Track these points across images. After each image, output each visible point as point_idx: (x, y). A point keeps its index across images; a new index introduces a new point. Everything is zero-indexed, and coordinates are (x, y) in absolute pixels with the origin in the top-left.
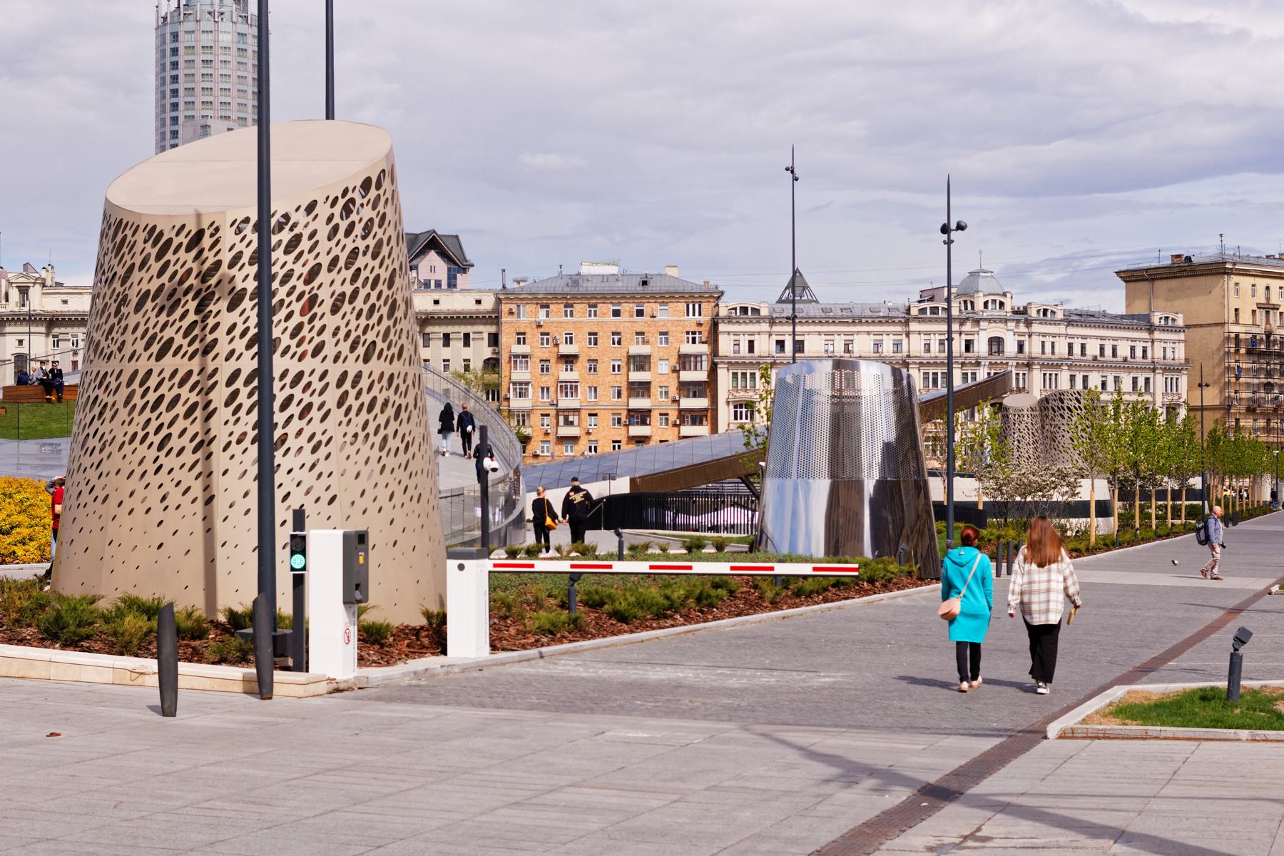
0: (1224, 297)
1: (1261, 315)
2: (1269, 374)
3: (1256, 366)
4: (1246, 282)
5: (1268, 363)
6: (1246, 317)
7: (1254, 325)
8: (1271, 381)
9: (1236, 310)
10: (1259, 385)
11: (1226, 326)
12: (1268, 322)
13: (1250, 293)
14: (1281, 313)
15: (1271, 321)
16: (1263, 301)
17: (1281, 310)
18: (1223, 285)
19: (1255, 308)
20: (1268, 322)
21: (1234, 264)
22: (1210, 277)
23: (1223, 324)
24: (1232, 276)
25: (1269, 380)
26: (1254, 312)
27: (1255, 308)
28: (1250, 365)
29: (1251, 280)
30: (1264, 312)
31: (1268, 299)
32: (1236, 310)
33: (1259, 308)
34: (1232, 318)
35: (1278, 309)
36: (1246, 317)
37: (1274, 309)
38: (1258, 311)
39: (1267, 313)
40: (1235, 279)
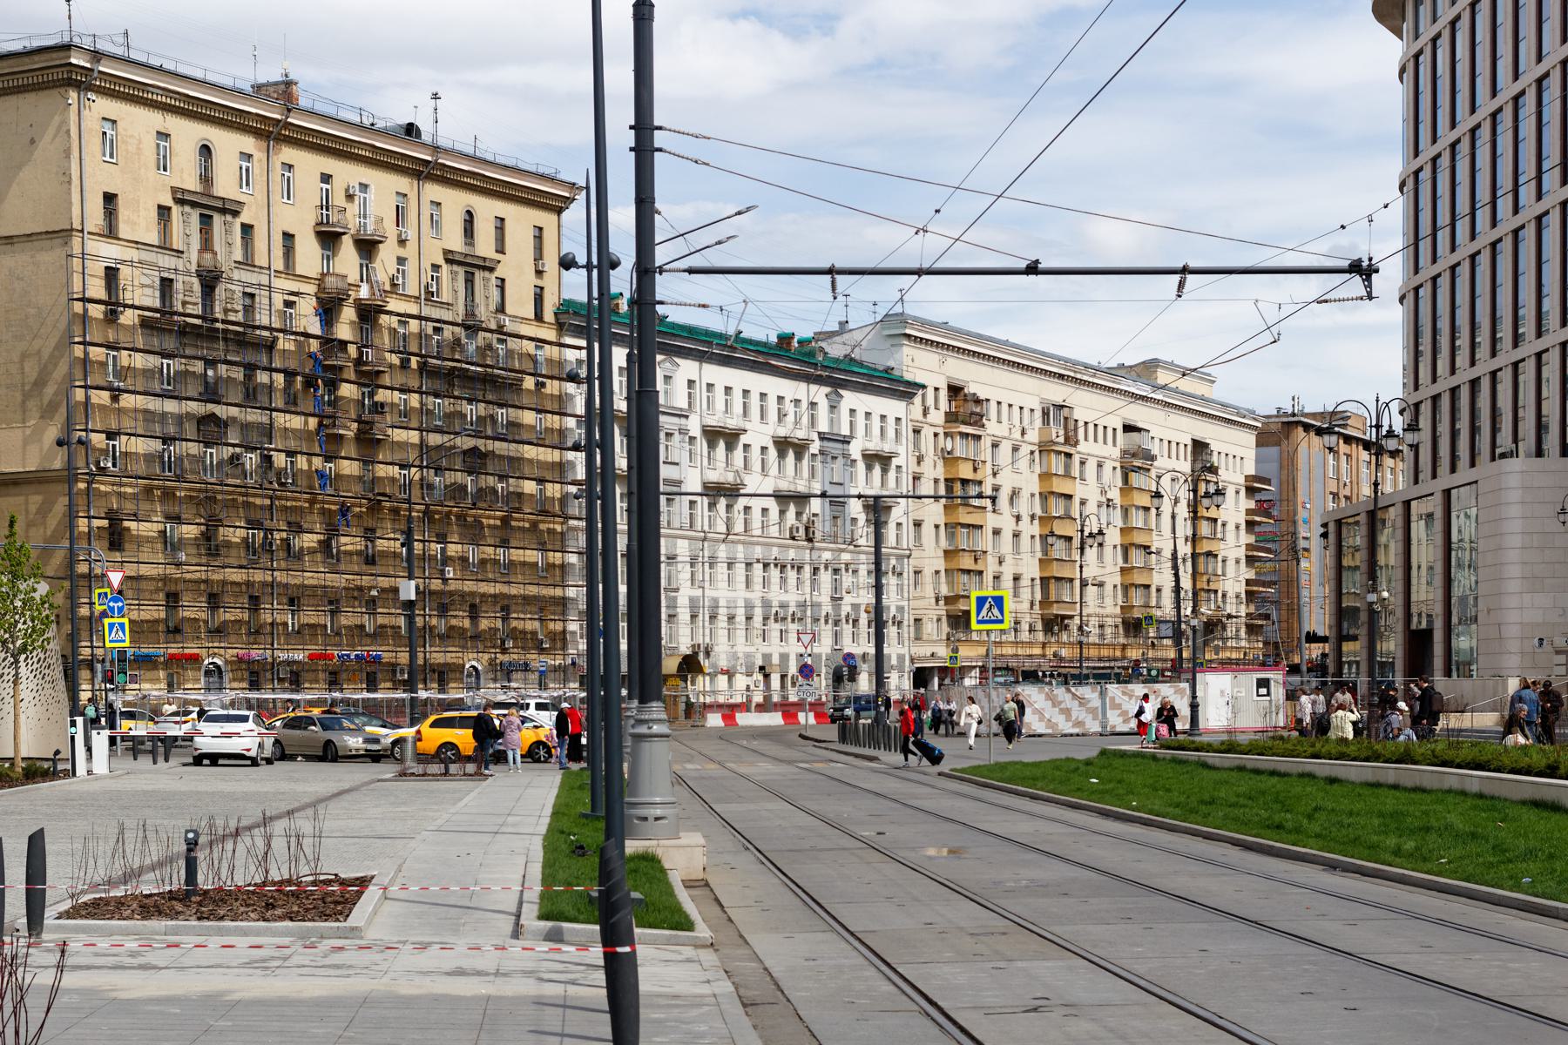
0: (67, 154)
1: (185, 225)
2: (211, 393)
3: (175, 365)
4: (139, 123)
5: (211, 363)
6: (138, 222)
7: (165, 247)
8: (221, 411)
9: (109, 198)
10: (180, 419)
11: (76, 241)
12: (207, 245)
13: (150, 156)
14: (247, 229)
15: (218, 245)
16: (192, 183)
17: (245, 217)
18: (65, 122)
19: (169, 202)
20: (207, 245)
21: (97, 55)
22: (31, 98)
23: (65, 234)
24: (90, 95)
25: (211, 407)
26: (163, 211)
27: (169, 202)
28: (153, 361)
29: (157, 120)
30: (195, 216)
31: (206, 179)
32: (109, 198)
33: (181, 202)
34: (95, 217)
35: (236, 214)
36: (138, 222)
37: (223, 211)
38: (176, 211)
39: (206, 220)
40: (103, 106)
